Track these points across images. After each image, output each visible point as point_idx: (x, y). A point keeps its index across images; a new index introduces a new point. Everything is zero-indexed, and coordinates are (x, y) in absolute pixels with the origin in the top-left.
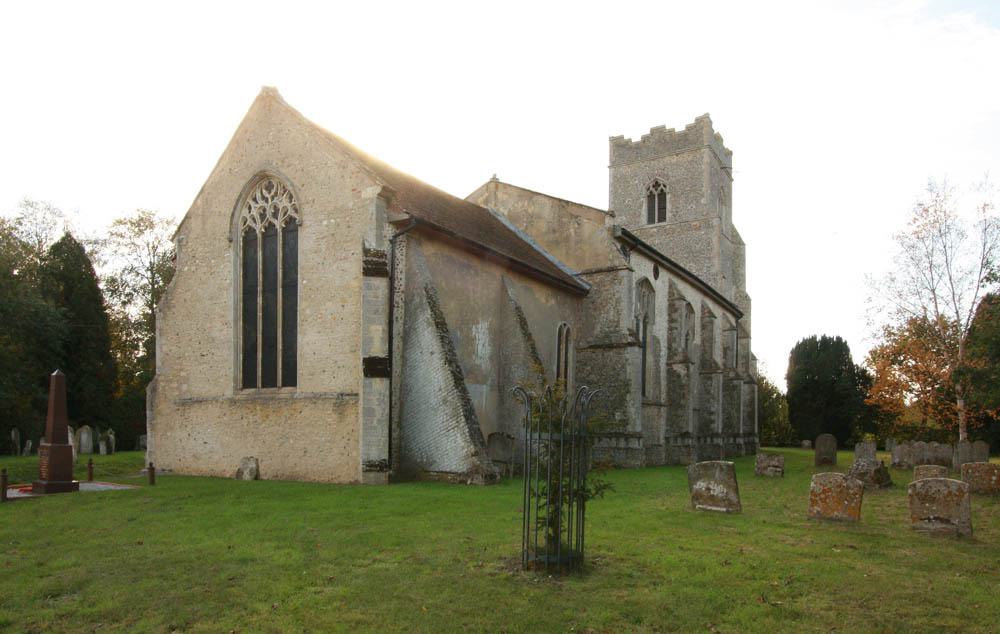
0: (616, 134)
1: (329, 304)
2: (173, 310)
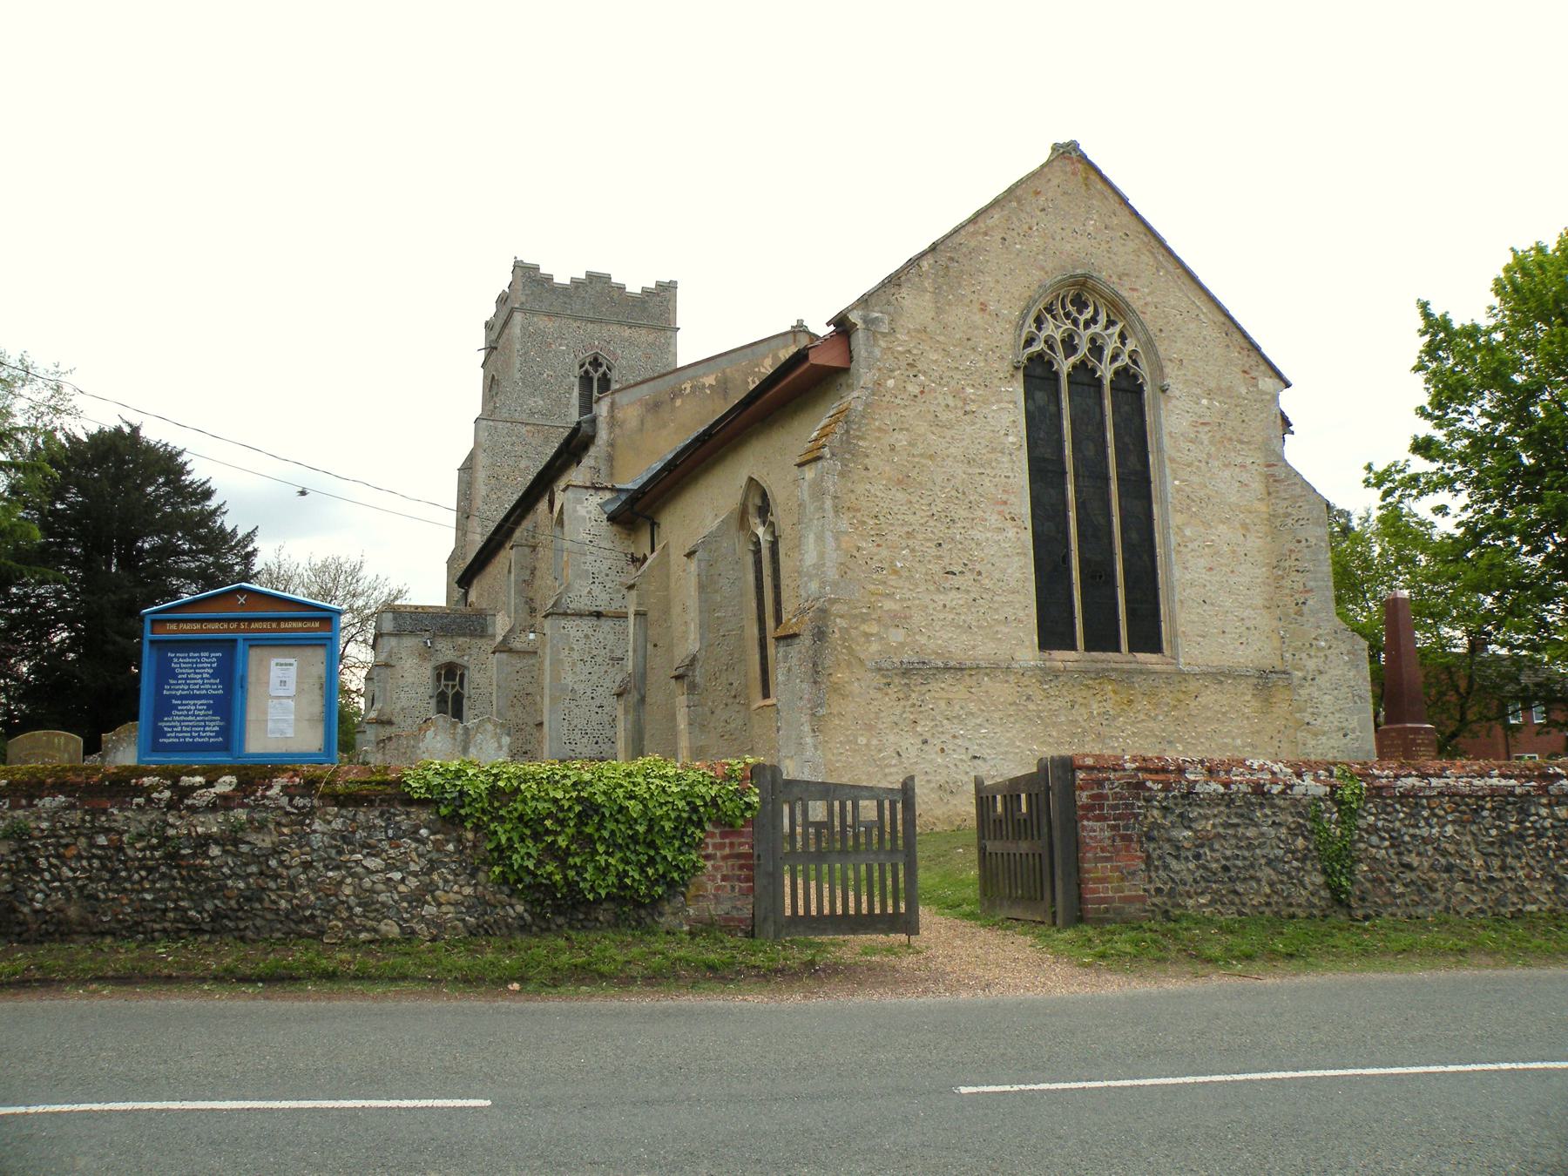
1: (1221, 526)
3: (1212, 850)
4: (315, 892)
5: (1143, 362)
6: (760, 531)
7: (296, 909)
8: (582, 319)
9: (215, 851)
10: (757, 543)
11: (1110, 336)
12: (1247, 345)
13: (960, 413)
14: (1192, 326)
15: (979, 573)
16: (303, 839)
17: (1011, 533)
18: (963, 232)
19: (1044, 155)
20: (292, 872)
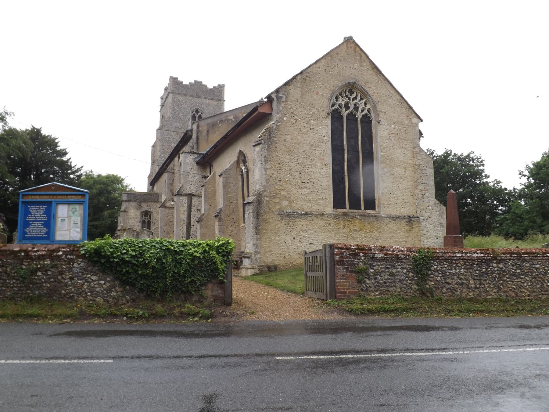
0: (174, 76)
1: (397, 168)
2: (276, 145)
3: (381, 276)
4: (74, 287)
5: (372, 112)
6: (243, 168)
7: (67, 293)
8: (192, 96)
9: (39, 273)
10: (242, 172)
11: (361, 103)
12: (408, 107)
13: (309, 129)
14: (390, 100)
15: (314, 183)
16: (70, 269)
17: (325, 170)
18: (311, 67)
19: (342, 41)
20: (66, 281)
